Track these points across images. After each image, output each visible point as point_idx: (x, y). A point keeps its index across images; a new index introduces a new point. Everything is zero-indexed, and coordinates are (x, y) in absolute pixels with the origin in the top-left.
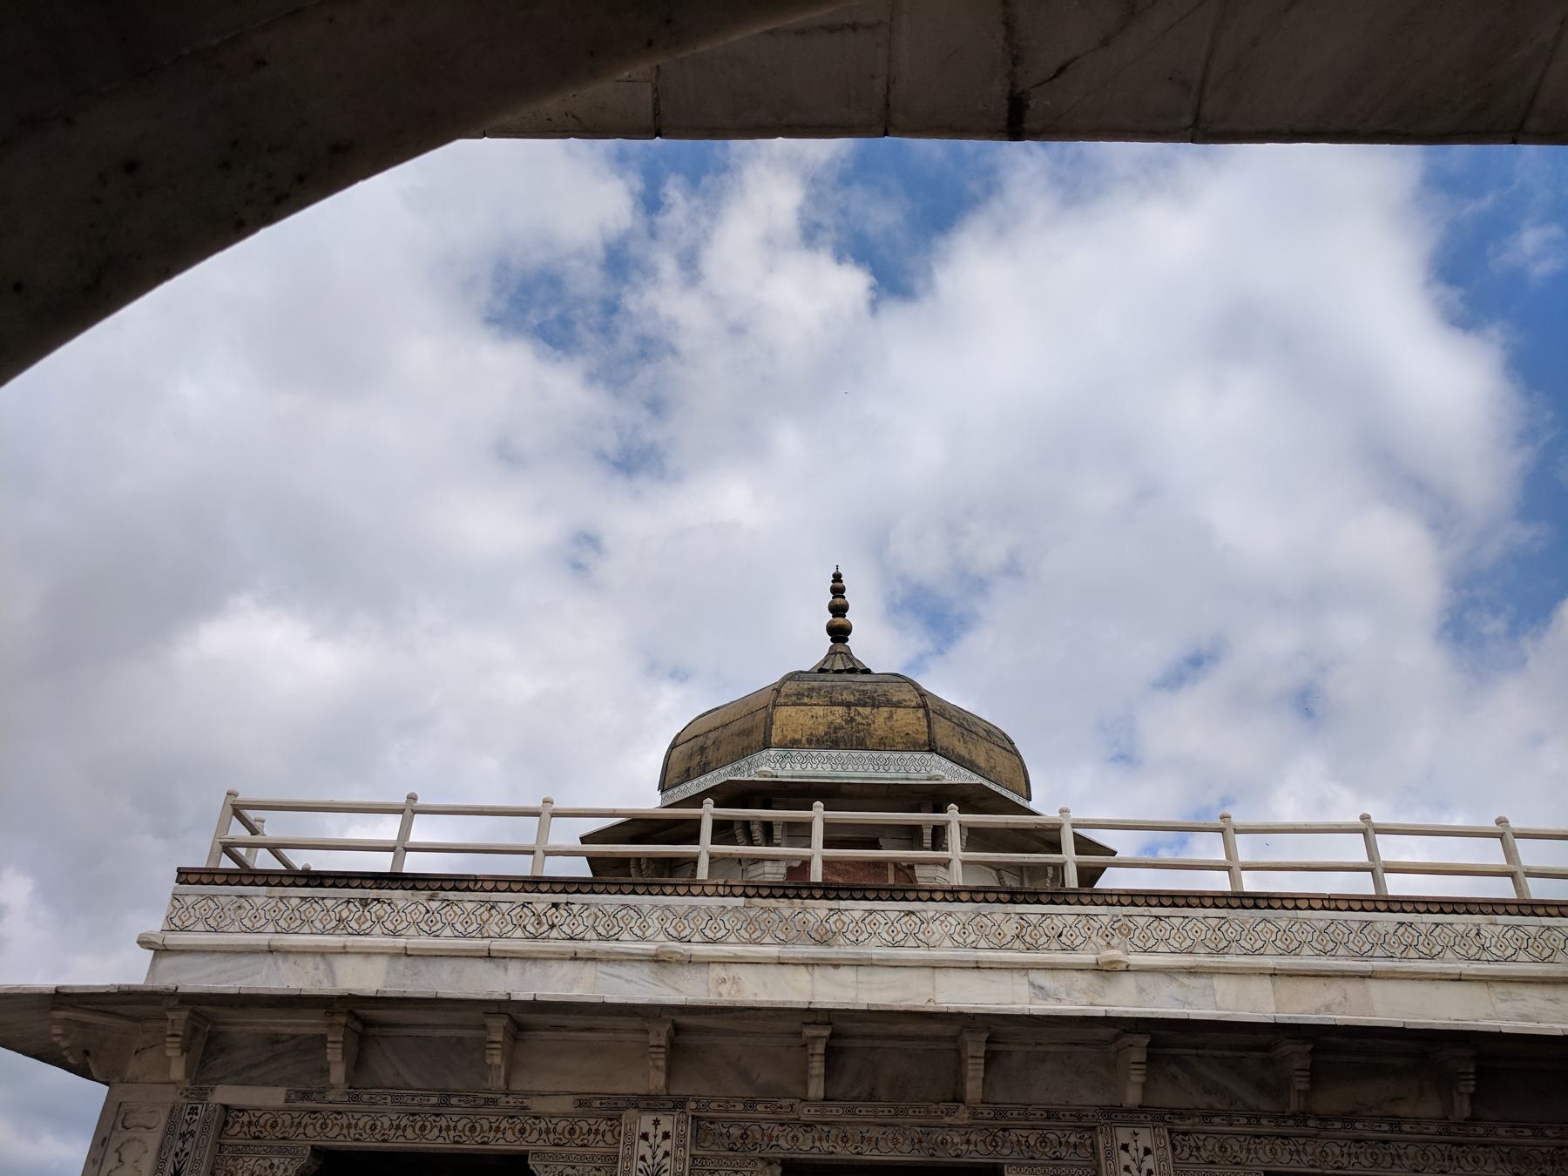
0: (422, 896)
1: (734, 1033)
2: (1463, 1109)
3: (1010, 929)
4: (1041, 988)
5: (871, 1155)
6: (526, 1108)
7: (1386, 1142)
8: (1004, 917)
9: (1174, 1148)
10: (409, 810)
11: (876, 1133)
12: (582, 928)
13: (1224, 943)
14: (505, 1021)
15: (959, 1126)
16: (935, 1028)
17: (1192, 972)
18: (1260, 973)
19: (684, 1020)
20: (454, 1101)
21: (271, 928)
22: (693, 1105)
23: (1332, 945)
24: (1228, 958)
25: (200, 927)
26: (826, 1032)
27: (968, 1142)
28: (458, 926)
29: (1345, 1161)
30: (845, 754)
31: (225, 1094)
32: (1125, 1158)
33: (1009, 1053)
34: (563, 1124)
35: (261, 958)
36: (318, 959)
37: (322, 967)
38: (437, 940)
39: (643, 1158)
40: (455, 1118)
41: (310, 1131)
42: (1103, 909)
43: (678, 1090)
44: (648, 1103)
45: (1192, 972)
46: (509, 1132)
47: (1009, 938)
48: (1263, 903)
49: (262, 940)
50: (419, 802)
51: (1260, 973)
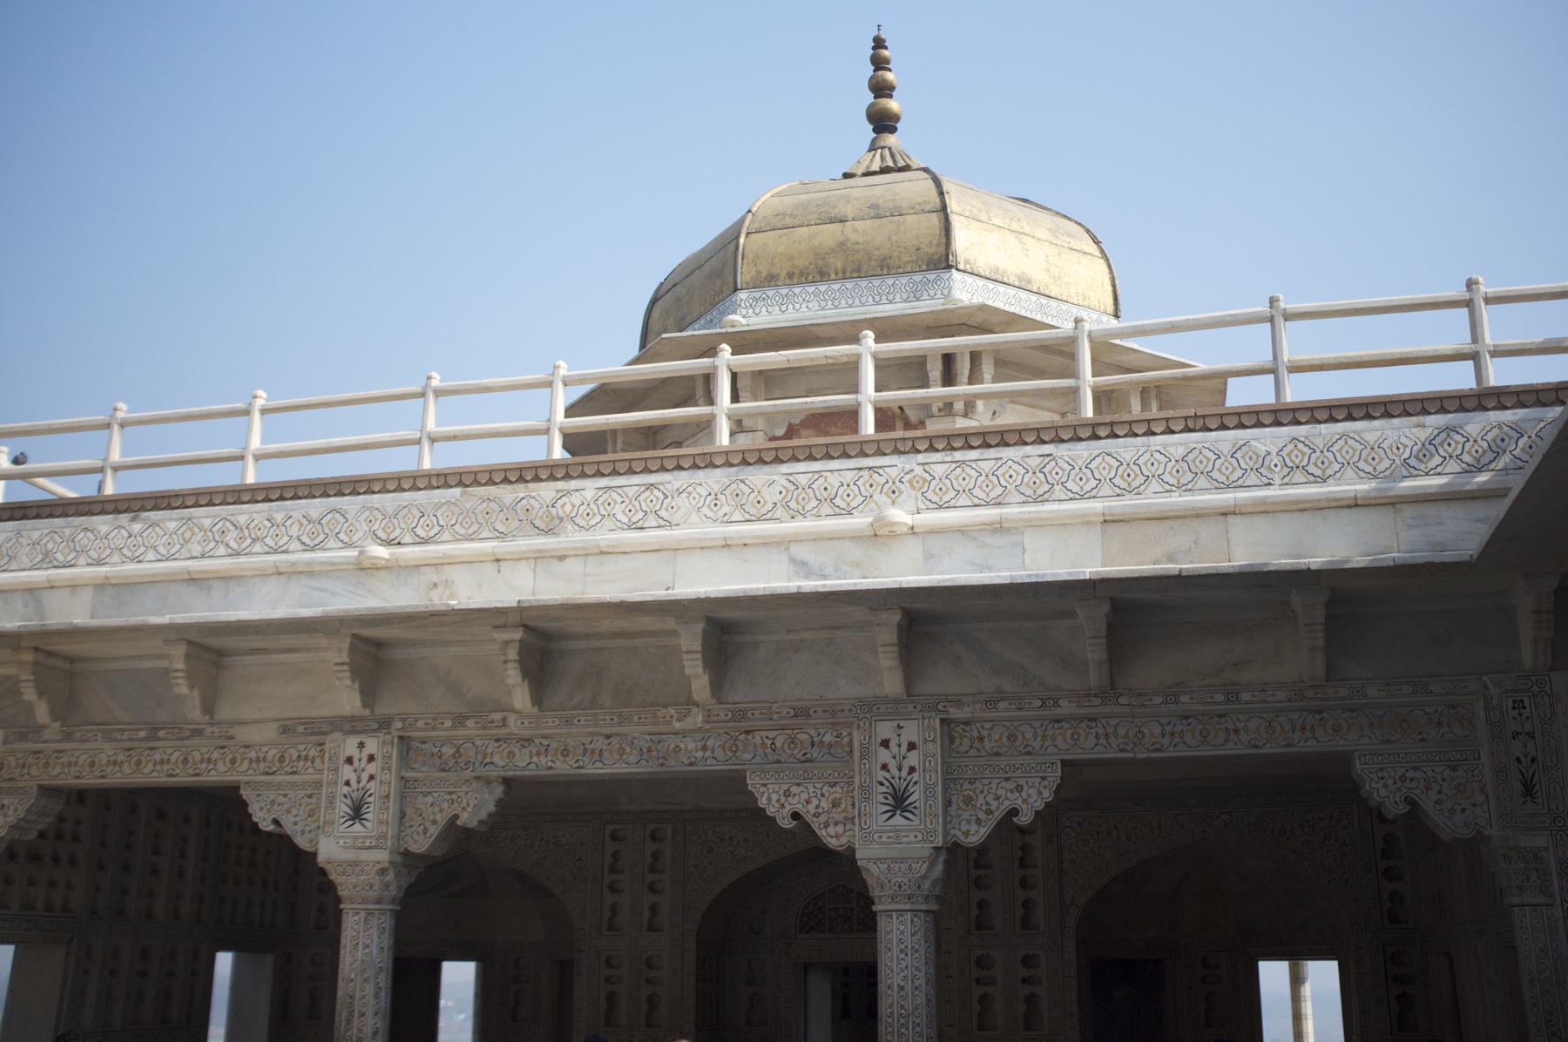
0: (124, 518)
3: (771, 496)
4: (804, 563)
5: (593, 769)
6: (231, 738)
7: (1221, 716)
11: (601, 743)
13: (1046, 487)
18: (1085, 521)
19: (365, 632)
22: (399, 725)
23: (1190, 476)
24: (1048, 507)
27: (705, 748)
32: (884, 756)
34: (273, 751)
38: (140, 566)
39: (347, 783)
41: (34, 771)
43: (383, 709)
44: (351, 725)
47: (769, 506)
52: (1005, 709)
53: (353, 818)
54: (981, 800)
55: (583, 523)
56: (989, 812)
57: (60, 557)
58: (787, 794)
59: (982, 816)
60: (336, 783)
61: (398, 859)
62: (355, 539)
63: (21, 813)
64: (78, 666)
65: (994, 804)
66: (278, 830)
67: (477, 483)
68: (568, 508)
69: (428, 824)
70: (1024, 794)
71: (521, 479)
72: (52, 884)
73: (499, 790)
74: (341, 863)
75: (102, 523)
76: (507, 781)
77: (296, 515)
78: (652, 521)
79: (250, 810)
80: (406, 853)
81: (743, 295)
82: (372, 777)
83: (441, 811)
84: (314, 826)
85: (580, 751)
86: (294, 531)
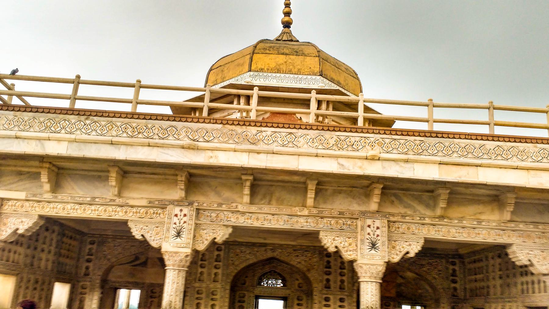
0: (83, 118)
1: (215, 177)
2: (507, 216)
3: (332, 142)
4: (343, 165)
8: (331, 137)
9: (389, 227)
10: (77, 82)
11: (270, 217)
12: (152, 134)
13: (421, 151)
14: (116, 169)
15: (304, 216)
16: (296, 178)
17: (407, 161)
18: (434, 163)
19: (193, 171)
20: (97, 200)
21: (16, 128)
22: (197, 204)
23: (466, 153)
26: (251, 178)
27: (307, 222)
28: (98, 131)
29: (457, 235)
30: (282, 75)
32: (369, 230)
33: (326, 190)
35: (13, 140)
36: (38, 142)
37: (39, 145)
41: (37, 209)
42: (372, 135)
44: (178, 203)
45: (407, 161)
48: (440, 135)
49: (13, 133)
50: (82, 78)
51: (434, 163)
52: (408, 219)
54: (398, 248)
55: (266, 143)
56: (400, 252)
58: (334, 240)
59: (398, 253)
60: (170, 223)
62: (180, 137)
63: (30, 224)
65: (402, 249)
67: (227, 123)
68: (261, 137)
69: (204, 240)
70: (412, 247)
71: (244, 125)
72: (15, 252)
73: (230, 230)
75: (73, 118)
76: (234, 227)
77: (157, 126)
78: (291, 145)
79: (132, 231)
81: (252, 73)
82: (185, 222)
84: (158, 238)
85: (263, 219)
86: (156, 131)
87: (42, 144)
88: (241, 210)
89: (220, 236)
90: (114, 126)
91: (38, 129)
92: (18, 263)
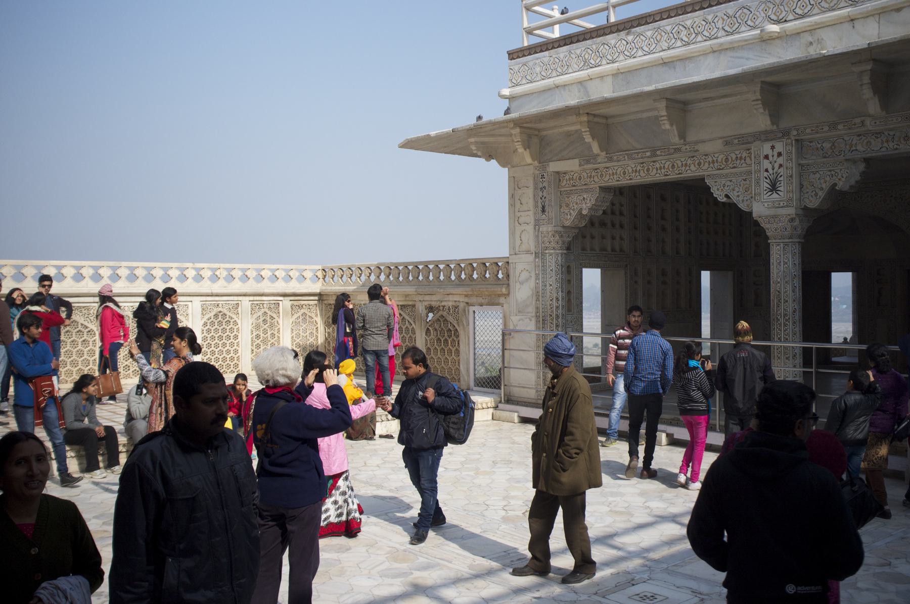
6: (697, 151)
19: (769, 79)
22: (795, 133)
25: (524, 81)
28: (645, 48)
31: (554, 167)
38: (635, 60)
39: (767, 170)
40: (663, 162)
41: (596, 179)
43: (784, 124)
44: (765, 136)
46: (692, 166)
53: (771, 191)
57: (592, 61)
61: (801, 212)
64: (610, 121)
66: (729, 201)
69: (817, 190)
72: (613, 238)
73: (862, 167)
74: (766, 217)
75: (611, 39)
76: (867, 160)
80: (805, 209)
83: (825, 182)
86: (720, 25)
87: (585, 88)
88: (871, 128)
89: (843, 179)
90: (663, 34)
91: (576, 66)
92: (621, 250)
